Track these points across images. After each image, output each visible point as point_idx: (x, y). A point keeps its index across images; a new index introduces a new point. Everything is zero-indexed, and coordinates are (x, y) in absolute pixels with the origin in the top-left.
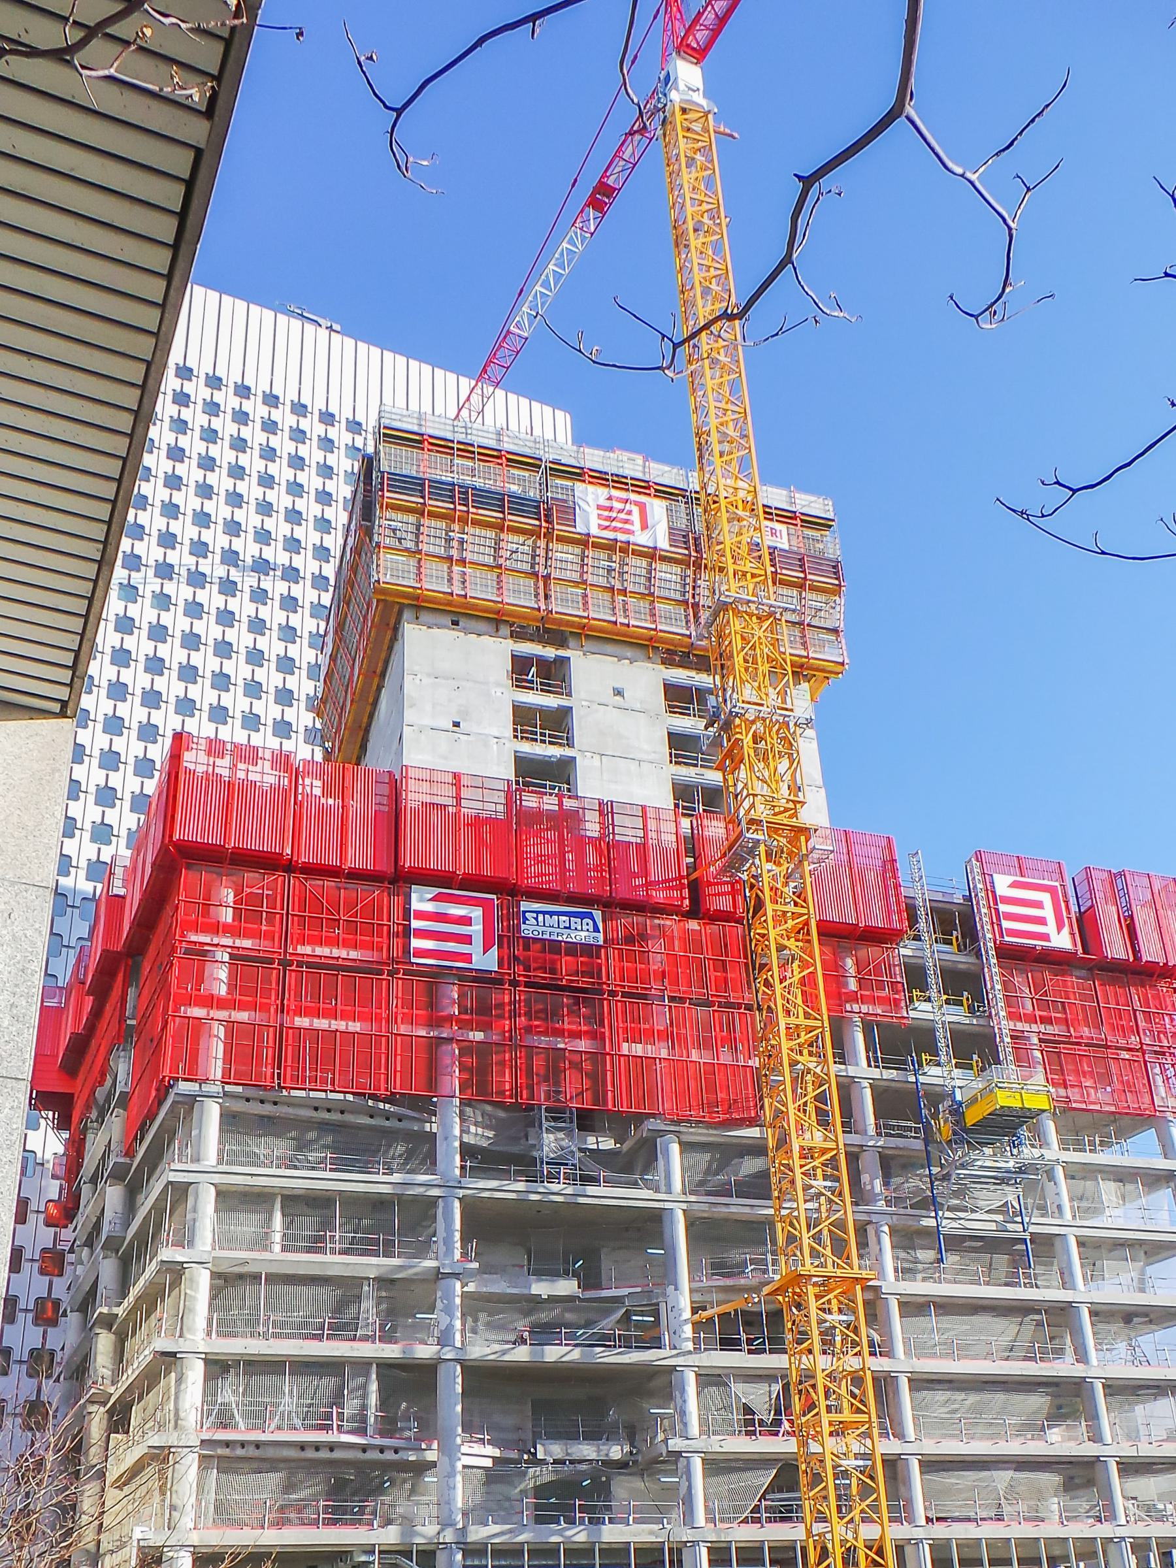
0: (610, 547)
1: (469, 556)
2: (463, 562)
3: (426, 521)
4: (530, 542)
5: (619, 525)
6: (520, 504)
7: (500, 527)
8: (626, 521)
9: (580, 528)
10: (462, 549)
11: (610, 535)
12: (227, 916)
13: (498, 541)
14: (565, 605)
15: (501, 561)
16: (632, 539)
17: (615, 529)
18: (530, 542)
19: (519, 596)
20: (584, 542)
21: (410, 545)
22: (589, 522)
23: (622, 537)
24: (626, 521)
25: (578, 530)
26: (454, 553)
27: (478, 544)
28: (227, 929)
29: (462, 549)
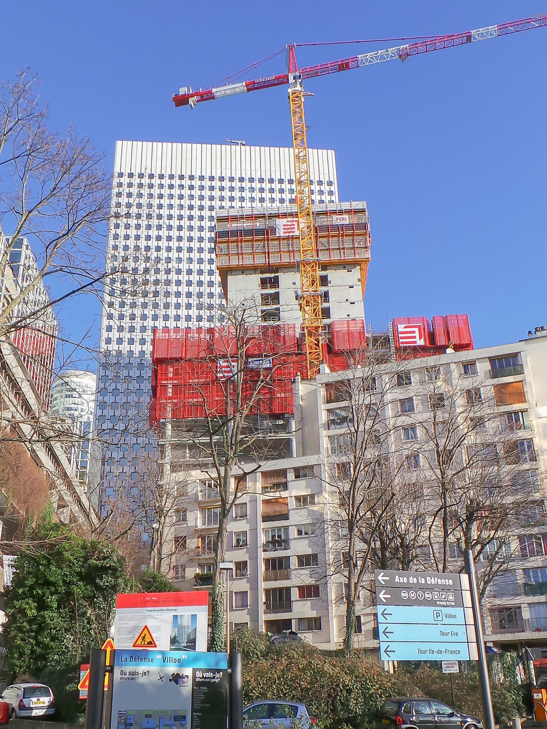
0: (288, 238)
1: (244, 252)
2: (242, 254)
3: (230, 244)
4: (262, 243)
5: (290, 230)
6: (258, 232)
7: (252, 241)
8: (292, 228)
9: (278, 235)
10: (242, 250)
11: (287, 235)
12: (171, 375)
13: (253, 245)
14: (274, 260)
15: (254, 251)
16: (294, 234)
17: (289, 232)
18: (262, 243)
19: (260, 260)
20: (279, 239)
21: (226, 253)
22: (281, 233)
23: (291, 234)
24: (292, 228)
25: (277, 235)
26: (240, 252)
27: (246, 248)
28: (171, 379)
29: (242, 250)
